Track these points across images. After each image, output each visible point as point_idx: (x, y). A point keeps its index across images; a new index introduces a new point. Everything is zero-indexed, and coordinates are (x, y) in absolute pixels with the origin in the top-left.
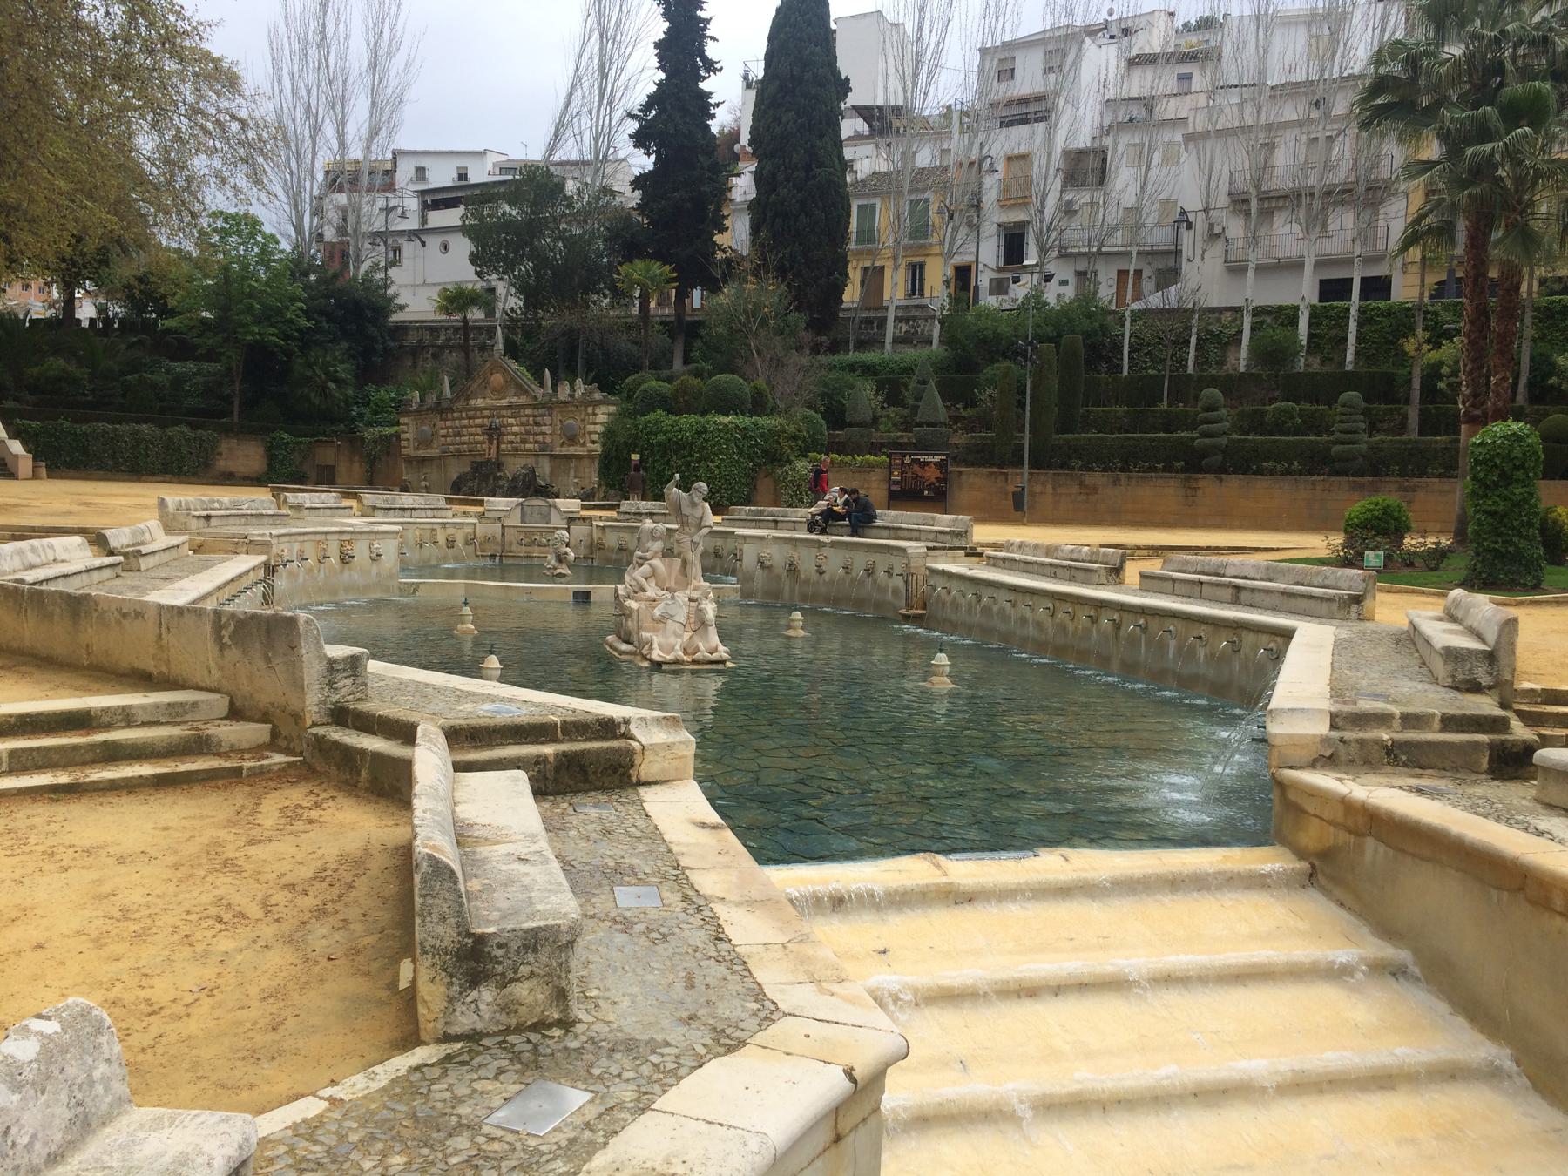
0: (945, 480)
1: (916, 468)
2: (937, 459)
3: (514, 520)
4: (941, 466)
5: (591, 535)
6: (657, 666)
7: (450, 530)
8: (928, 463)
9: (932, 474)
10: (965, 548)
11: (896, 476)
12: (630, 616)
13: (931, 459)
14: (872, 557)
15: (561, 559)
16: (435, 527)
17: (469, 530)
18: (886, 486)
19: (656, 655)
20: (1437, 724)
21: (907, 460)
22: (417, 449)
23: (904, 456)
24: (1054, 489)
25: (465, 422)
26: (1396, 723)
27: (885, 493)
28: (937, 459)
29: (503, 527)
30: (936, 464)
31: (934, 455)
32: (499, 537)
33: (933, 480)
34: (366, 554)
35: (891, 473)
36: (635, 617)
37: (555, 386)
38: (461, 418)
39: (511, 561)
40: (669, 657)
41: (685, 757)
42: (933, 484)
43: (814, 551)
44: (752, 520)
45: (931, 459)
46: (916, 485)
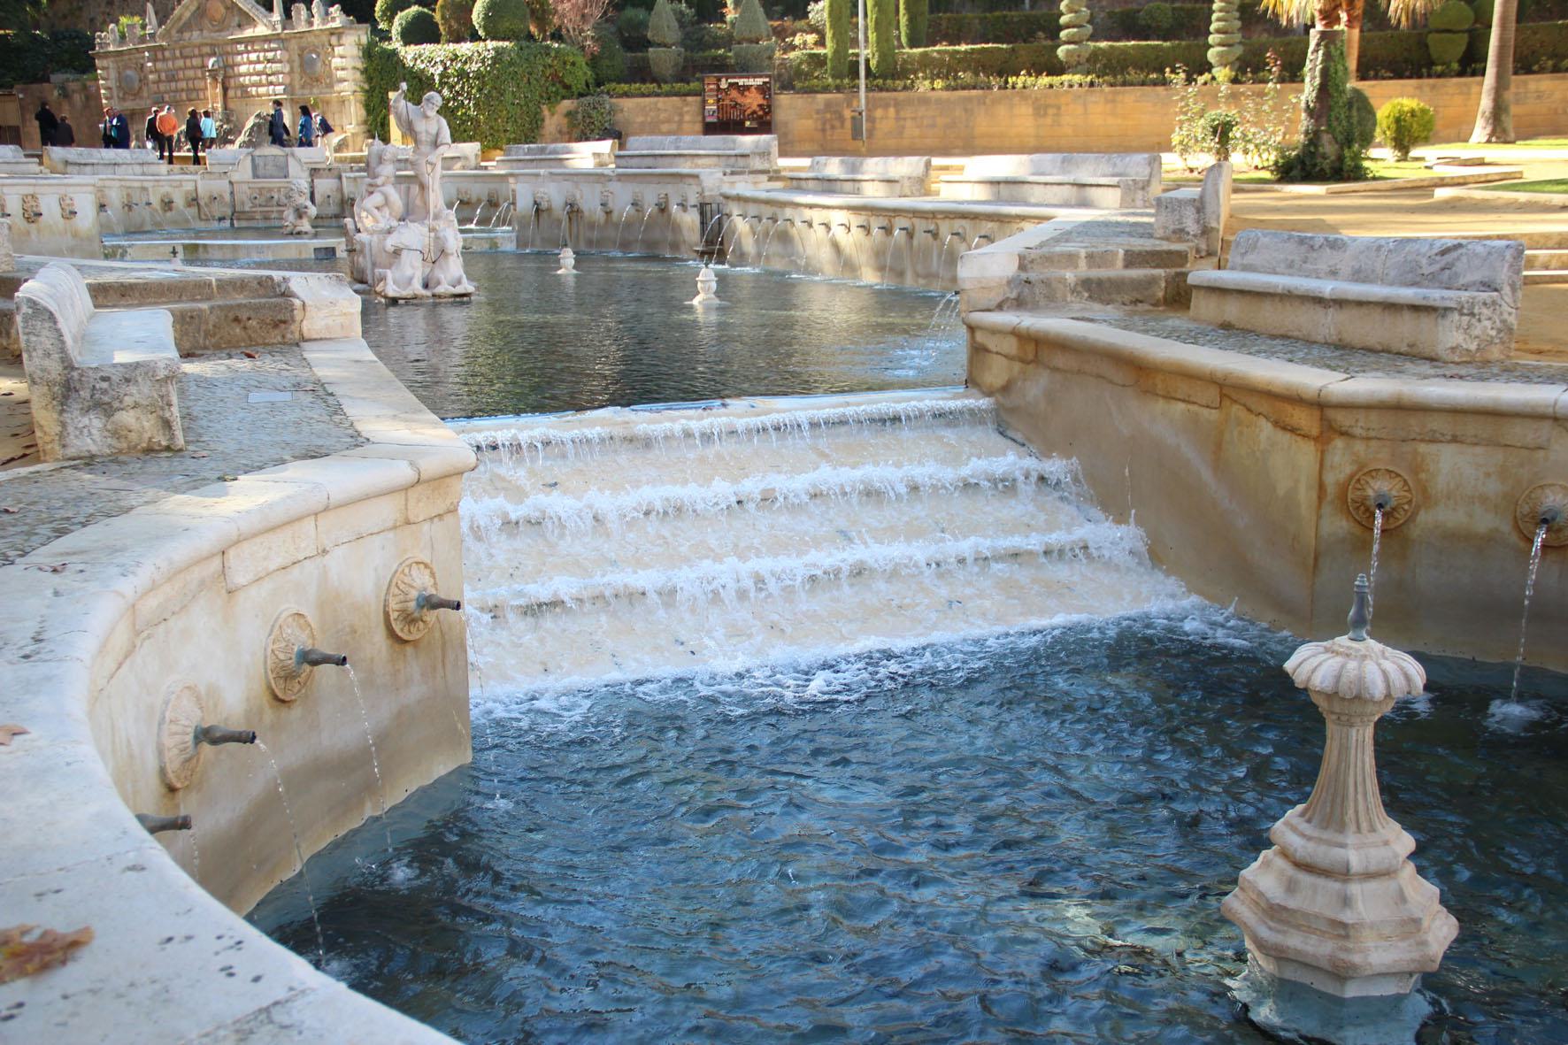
0: (769, 106)
1: (734, 94)
2: (759, 81)
3: (243, 173)
4: (763, 90)
5: (340, 189)
6: (394, 302)
7: (166, 189)
8: (747, 88)
9: (753, 101)
10: (768, 172)
11: (711, 106)
12: (362, 251)
13: (751, 82)
14: (663, 189)
15: (300, 213)
16: (145, 184)
17: (190, 187)
18: (700, 118)
19: (392, 291)
20: (1120, 263)
21: (724, 85)
22: (124, 99)
23: (719, 80)
24: (897, 112)
25: (180, 63)
26: (1082, 263)
28: (759, 81)
29: (231, 183)
30: (759, 88)
31: (755, 77)
32: (227, 197)
33: (755, 107)
34: (57, 211)
35: (704, 102)
36: (367, 251)
37: (287, 13)
38: (174, 58)
39: (244, 224)
40: (405, 293)
41: (352, 314)
42: (754, 112)
43: (599, 187)
44: (532, 160)
45: (751, 82)
46: (735, 115)
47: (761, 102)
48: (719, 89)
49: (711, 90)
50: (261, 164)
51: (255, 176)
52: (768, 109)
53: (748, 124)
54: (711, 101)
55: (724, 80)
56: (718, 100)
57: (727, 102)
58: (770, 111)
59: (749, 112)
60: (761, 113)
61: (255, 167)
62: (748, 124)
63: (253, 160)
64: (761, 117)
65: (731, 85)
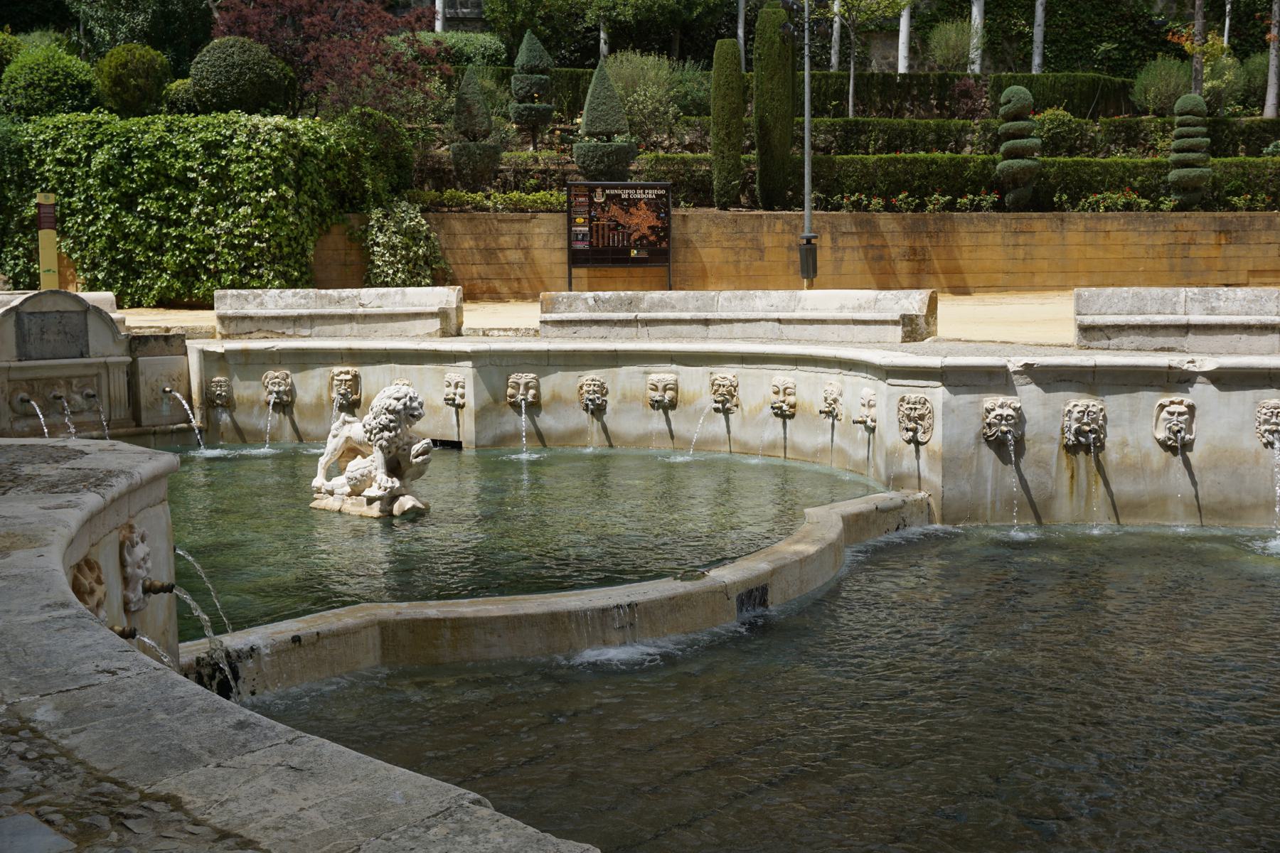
0: (667, 229)
1: (615, 210)
2: (651, 194)
4: (654, 205)
8: (634, 203)
9: (642, 220)
13: (639, 194)
18: (562, 243)
21: (599, 199)
23: (592, 190)
24: (834, 240)
27: (562, 257)
28: (651, 194)
30: (649, 203)
35: (571, 222)
45: (639, 194)
46: (616, 240)
47: (654, 223)
48: (591, 203)
49: (581, 204)
50: (35, 330)
51: (23, 356)
52: (663, 232)
53: (634, 253)
54: (580, 220)
55: (599, 191)
56: (591, 219)
57: (604, 222)
58: (667, 236)
59: (636, 236)
60: (652, 238)
61: (22, 338)
62: (634, 253)
63: (19, 323)
64: (650, 243)
65: (609, 197)
